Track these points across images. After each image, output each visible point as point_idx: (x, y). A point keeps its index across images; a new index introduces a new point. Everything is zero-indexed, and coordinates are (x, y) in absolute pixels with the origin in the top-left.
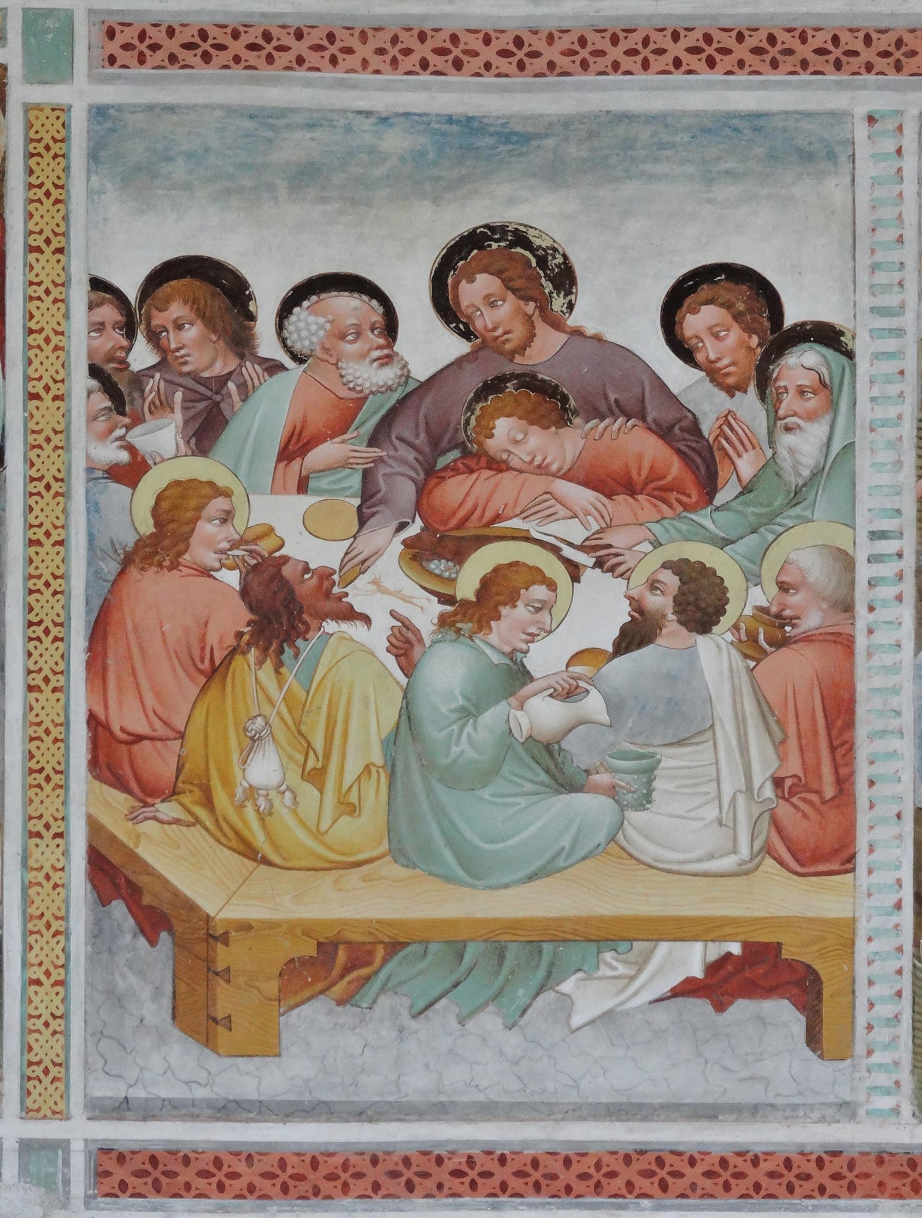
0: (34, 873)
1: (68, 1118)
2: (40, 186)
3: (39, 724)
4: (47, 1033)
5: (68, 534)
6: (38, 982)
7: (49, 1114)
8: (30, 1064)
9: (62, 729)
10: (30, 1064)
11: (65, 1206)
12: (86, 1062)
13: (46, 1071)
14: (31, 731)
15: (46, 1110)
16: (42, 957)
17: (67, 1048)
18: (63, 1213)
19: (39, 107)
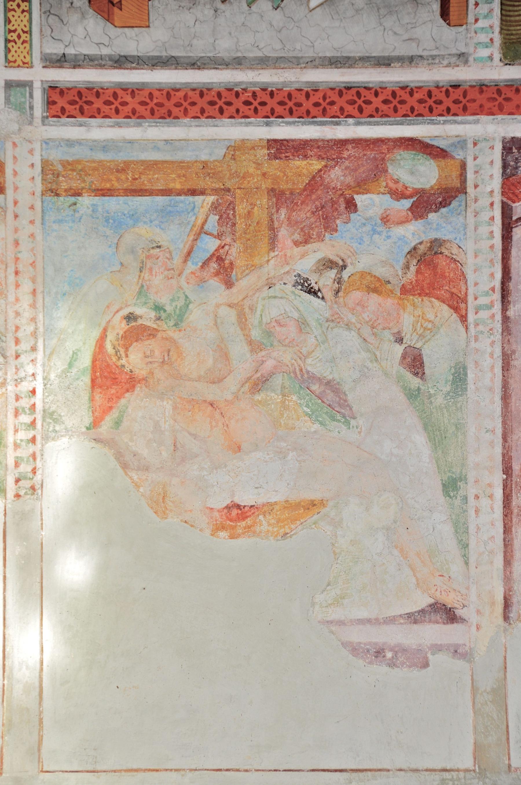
1: (32, 67)
4: (19, 11)
7: (21, 64)
8: (10, 31)
10: (10, 31)
11: (31, 123)
12: (41, 31)
13: (19, 37)
15: (19, 62)
17: (30, 21)
18: (30, 128)
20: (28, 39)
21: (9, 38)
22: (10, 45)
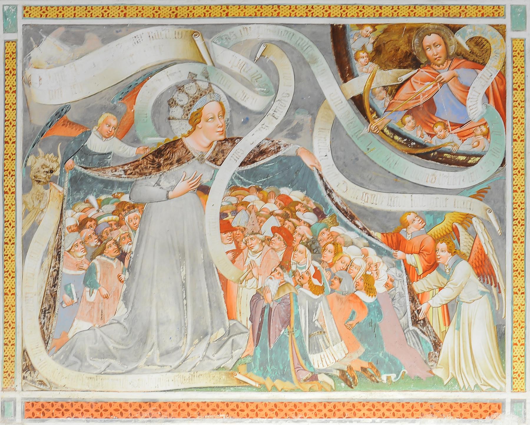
0: (515, 306)
3: (517, 254)
5: (525, 188)
6: (516, 344)
7: (520, 390)
8: (514, 373)
9: (523, 256)
10: (514, 373)
14: (514, 257)
16: (517, 335)
20: (524, 377)
21: (514, 376)
22: (514, 380)
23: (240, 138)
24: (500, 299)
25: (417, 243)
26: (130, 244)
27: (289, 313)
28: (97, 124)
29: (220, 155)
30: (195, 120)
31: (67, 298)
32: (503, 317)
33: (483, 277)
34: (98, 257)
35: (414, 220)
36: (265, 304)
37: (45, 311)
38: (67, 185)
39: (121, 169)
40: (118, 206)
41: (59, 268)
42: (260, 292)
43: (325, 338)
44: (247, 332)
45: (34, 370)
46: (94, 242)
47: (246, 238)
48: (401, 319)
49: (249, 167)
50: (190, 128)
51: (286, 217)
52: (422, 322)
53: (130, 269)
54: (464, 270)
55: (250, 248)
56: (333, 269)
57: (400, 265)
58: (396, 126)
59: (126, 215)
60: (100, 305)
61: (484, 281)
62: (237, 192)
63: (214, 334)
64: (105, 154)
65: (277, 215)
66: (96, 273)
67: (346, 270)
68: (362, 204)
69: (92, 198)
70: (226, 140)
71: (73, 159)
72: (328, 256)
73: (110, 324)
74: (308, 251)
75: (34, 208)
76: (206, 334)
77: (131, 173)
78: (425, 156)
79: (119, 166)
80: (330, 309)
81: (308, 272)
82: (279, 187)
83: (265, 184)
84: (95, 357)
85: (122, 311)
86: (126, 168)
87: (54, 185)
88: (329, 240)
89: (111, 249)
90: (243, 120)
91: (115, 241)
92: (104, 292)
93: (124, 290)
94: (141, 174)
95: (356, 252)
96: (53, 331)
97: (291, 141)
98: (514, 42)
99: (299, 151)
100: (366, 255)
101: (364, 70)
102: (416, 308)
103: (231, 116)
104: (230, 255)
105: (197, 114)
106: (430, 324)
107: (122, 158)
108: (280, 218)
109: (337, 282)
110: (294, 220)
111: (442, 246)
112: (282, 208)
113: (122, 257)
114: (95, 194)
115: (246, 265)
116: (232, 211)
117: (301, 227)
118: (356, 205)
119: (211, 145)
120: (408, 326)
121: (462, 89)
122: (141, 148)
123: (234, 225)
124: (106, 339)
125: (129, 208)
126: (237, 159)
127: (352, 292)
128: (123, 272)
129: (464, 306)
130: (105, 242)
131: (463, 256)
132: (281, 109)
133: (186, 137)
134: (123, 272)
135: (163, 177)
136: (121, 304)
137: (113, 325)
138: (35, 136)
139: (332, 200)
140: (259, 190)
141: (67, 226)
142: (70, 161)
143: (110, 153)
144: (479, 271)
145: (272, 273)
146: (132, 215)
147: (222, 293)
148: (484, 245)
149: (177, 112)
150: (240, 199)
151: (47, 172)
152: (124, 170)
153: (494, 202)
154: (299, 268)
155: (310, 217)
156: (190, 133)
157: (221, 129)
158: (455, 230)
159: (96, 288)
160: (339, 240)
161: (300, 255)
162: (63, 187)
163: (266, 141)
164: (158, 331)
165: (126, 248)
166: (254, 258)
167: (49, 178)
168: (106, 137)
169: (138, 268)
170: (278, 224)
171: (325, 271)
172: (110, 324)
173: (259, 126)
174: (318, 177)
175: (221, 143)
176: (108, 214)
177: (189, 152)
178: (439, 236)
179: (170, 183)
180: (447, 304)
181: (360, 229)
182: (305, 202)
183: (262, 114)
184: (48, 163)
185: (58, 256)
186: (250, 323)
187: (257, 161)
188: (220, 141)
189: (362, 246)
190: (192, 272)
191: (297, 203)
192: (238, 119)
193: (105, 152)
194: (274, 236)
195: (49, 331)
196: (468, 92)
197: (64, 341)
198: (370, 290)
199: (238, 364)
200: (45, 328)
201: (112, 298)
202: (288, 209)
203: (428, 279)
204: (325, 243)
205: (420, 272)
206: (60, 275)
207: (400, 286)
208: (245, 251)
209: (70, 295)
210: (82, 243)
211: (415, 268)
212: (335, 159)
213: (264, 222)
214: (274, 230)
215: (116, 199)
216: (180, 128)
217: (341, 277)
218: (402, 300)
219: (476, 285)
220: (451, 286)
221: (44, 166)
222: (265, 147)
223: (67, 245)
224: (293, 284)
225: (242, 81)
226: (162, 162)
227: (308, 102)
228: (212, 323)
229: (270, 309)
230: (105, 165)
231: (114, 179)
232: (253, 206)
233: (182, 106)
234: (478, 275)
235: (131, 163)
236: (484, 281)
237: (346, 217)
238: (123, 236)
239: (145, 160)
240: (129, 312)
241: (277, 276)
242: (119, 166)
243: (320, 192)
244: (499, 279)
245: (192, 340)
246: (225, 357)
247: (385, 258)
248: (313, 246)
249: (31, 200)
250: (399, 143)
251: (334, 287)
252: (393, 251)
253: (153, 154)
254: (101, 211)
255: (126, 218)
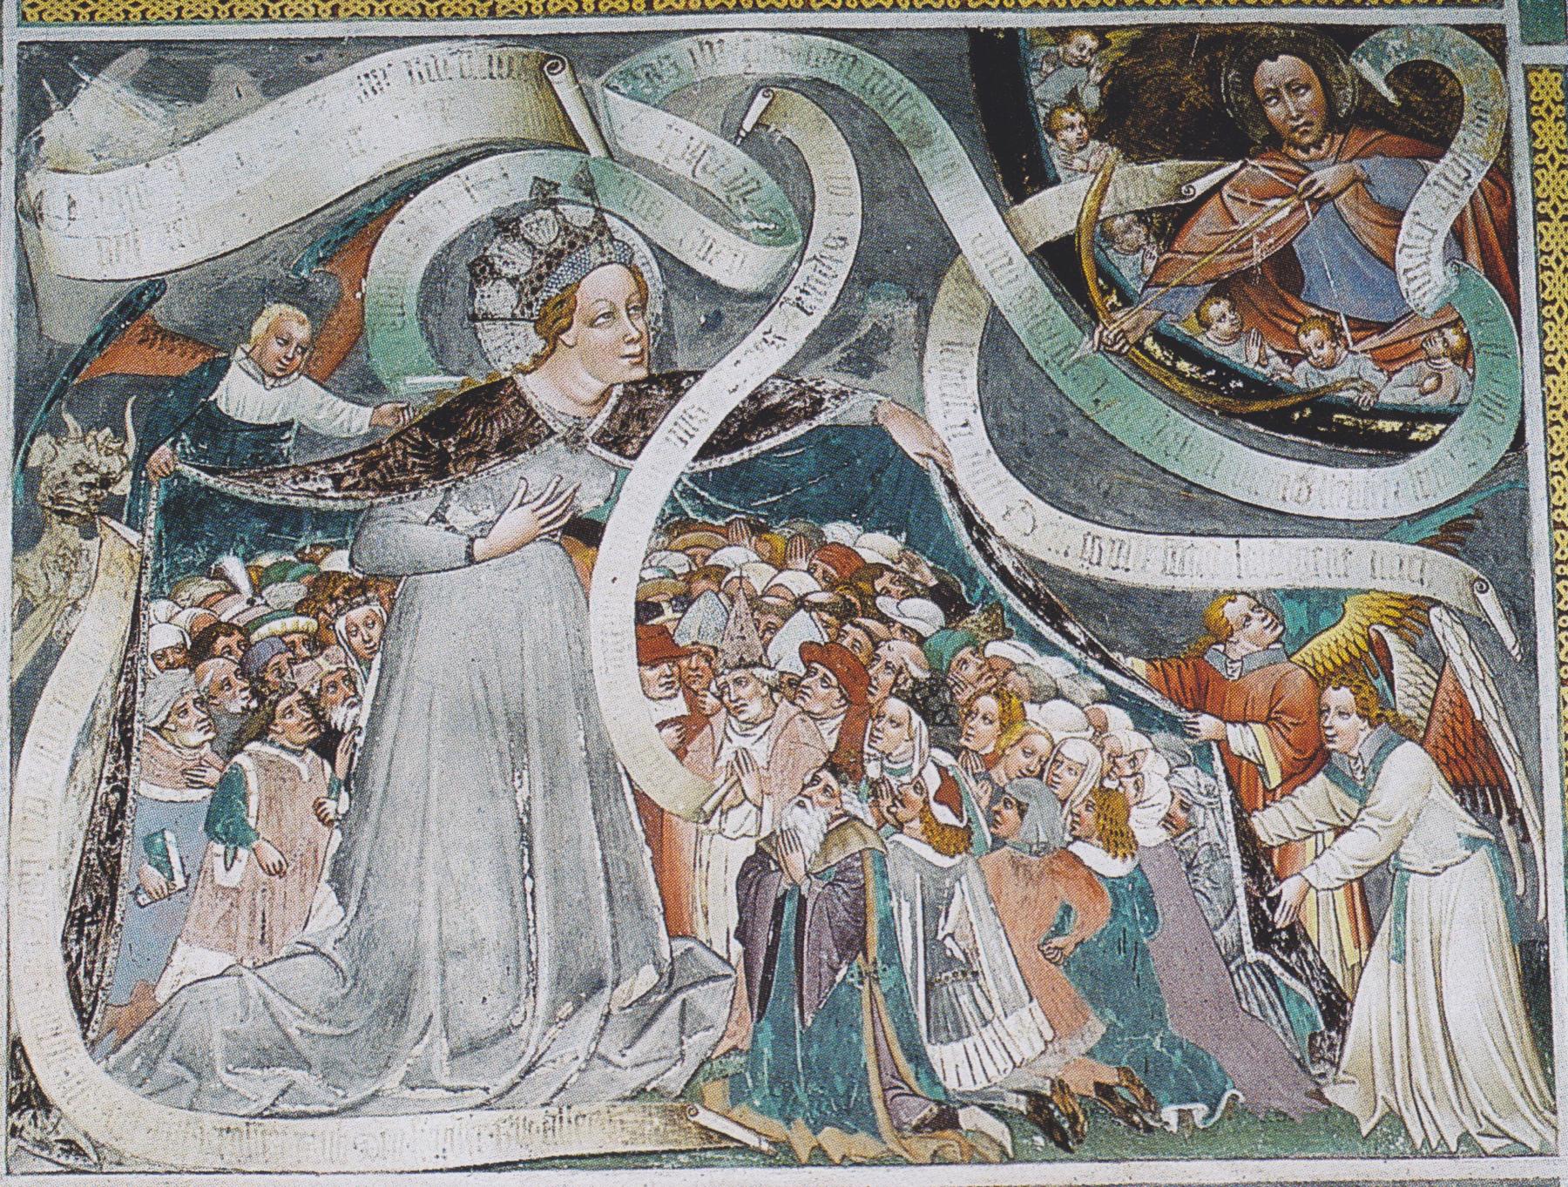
2: (1545, 150)
19: (1536, 68)
23: (698, 375)
24: (1528, 861)
25: (1259, 688)
26: (352, 705)
27: (859, 912)
28: (247, 340)
29: (635, 426)
30: (553, 321)
31: (154, 878)
32: (1541, 917)
33: (1472, 790)
34: (254, 746)
35: (1249, 618)
36: (785, 885)
37: (82, 919)
38: (152, 522)
39: (322, 472)
40: (313, 586)
41: (126, 781)
42: (768, 850)
43: (977, 991)
44: (728, 976)
45: (45, 1105)
46: (238, 701)
47: (721, 680)
48: (1216, 928)
49: (727, 460)
50: (538, 345)
51: (845, 613)
52: (1284, 935)
53: (354, 781)
54: (1410, 773)
55: (734, 711)
56: (998, 774)
57: (1210, 758)
58: (1185, 329)
59: (339, 613)
60: (259, 896)
61: (1474, 803)
62: (691, 537)
63: (624, 986)
64: (274, 426)
65: (820, 606)
66: (244, 798)
67: (1040, 777)
68: (1084, 572)
69: (232, 565)
70: (651, 380)
71: (173, 445)
72: (981, 734)
73: (288, 957)
74: (917, 719)
75: (48, 596)
76: (599, 985)
77: (354, 487)
78: (1278, 421)
79: (317, 464)
80: (991, 899)
81: (919, 787)
82: (822, 522)
83: (775, 513)
84: (245, 1063)
85: (327, 914)
86: (339, 468)
87: (113, 523)
88: (982, 685)
89: (293, 724)
90: (703, 320)
91: (306, 694)
92: (272, 857)
93: (333, 850)
94: (385, 488)
95: (1067, 720)
96: (106, 980)
97: (854, 380)
98: (1531, 76)
99: (882, 410)
100: (1101, 729)
101: (1078, 163)
102: (1264, 894)
103: (666, 308)
104: (671, 732)
105: (561, 302)
106: (1309, 941)
107: (327, 439)
108: (826, 617)
109: (1011, 814)
110: (871, 624)
111: (1340, 697)
112: (831, 586)
113: (326, 743)
114: (241, 550)
115: (722, 763)
116: (676, 597)
117: (892, 644)
118: (1064, 573)
119: (605, 395)
120: (1241, 951)
121: (1374, 217)
122: (387, 408)
123: (683, 642)
124: (278, 1004)
125: (347, 591)
126: (686, 437)
127: (1057, 843)
128: (330, 790)
129: (1416, 885)
130: (274, 697)
131: (1404, 731)
132: (823, 285)
133: (526, 372)
134: (333, 789)
135: (454, 495)
136: (325, 895)
137: (299, 959)
138: (54, 374)
139: (990, 558)
140: (758, 530)
141: (151, 651)
142: (165, 449)
143: (288, 425)
144: (1457, 774)
145: (804, 787)
146: (358, 614)
147: (648, 852)
148: (1470, 693)
149: (499, 298)
150: (699, 559)
151: (91, 485)
152: (332, 477)
153: (1496, 558)
154: (892, 771)
155: (924, 614)
156: (538, 360)
157: (636, 349)
158: (1378, 648)
159: (246, 843)
160: (1015, 681)
161: (892, 731)
162: (142, 531)
163: (779, 382)
164: (444, 976)
165: (339, 716)
166: (747, 743)
167: (96, 503)
168: (273, 375)
169: (378, 776)
170: (819, 636)
171: (972, 782)
172: (288, 957)
173: (756, 336)
174: (942, 490)
175: (635, 391)
176: (283, 613)
177: (538, 418)
178: (1329, 666)
179: (475, 513)
180: (1360, 880)
181: (1082, 647)
182: (903, 567)
183: (765, 299)
184: (95, 459)
185: (123, 746)
186: (737, 948)
187: (750, 443)
188: (635, 383)
189: (1085, 700)
190: (551, 788)
191: (880, 569)
192: (689, 316)
193: (274, 420)
194: (808, 674)
195: (95, 980)
196: (1399, 227)
197: (143, 1010)
198: (1118, 839)
199: (700, 1079)
200: (81, 970)
201: (297, 876)
202: (850, 585)
203: (1299, 803)
204: (970, 691)
205: (1275, 778)
206: (130, 803)
207: (1211, 824)
208: (719, 720)
209: (164, 865)
210: (200, 702)
211: (1260, 769)
212: (996, 434)
213: (777, 629)
214: (808, 652)
215: (307, 566)
216: (507, 346)
217: (1023, 799)
218: (1219, 868)
219: (1449, 819)
220: (1369, 821)
221: (82, 466)
222: (776, 399)
223: (151, 710)
224: (871, 821)
225: (701, 201)
226: (451, 449)
227: (907, 258)
228: (616, 947)
229: (802, 901)
230: (274, 461)
231: (303, 502)
232: (741, 578)
233: (513, 281)
234: (1456, 787)
235: (353, 454)
236: (1474, 803)
237: (1034, 610)
238: (331, 678)
239: (398, 444)
240: (347, 921)
241: (823, 799)
242: (317, 464)
243: (950, 536)
244: (1522, 796)
245: (555, 1005)
246: (660, 1056)
247: (1161, 738)
248: (935, 704)
249: (40, 572)
250: (1192, 382)
251: (1002, 831)
252: (1184, 714)
253: (424, 425)
254: (259, 601)
255: (341, 624)
